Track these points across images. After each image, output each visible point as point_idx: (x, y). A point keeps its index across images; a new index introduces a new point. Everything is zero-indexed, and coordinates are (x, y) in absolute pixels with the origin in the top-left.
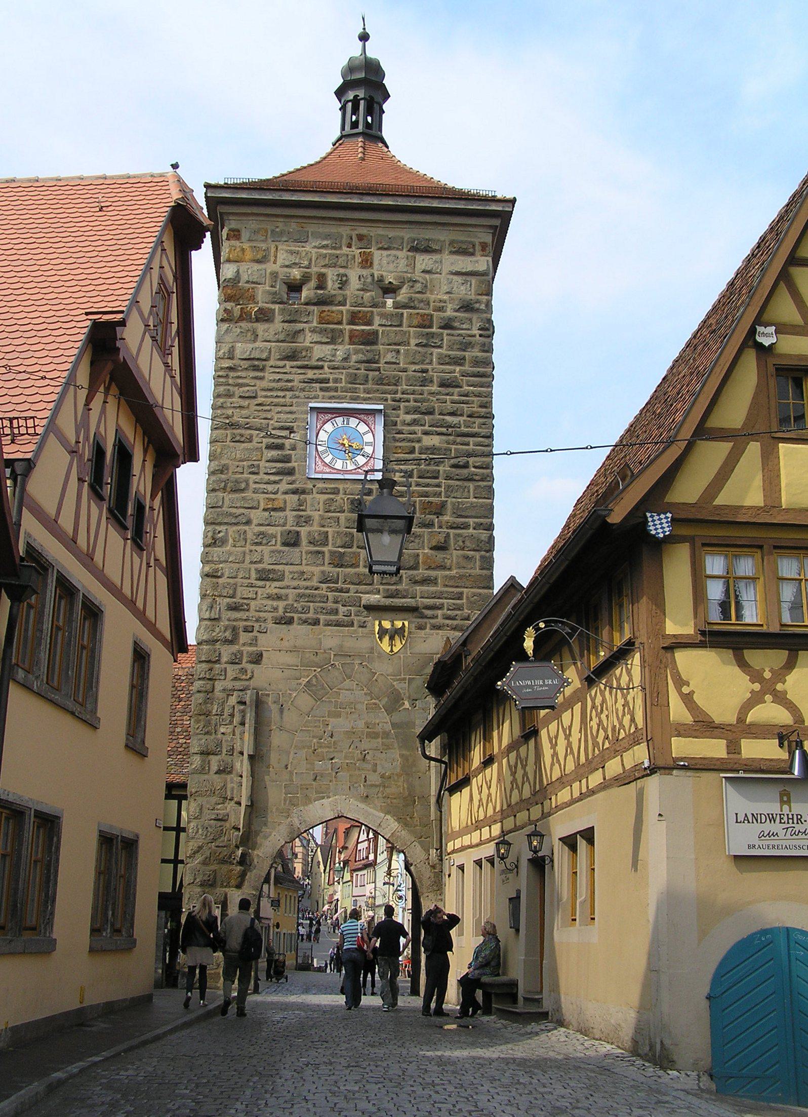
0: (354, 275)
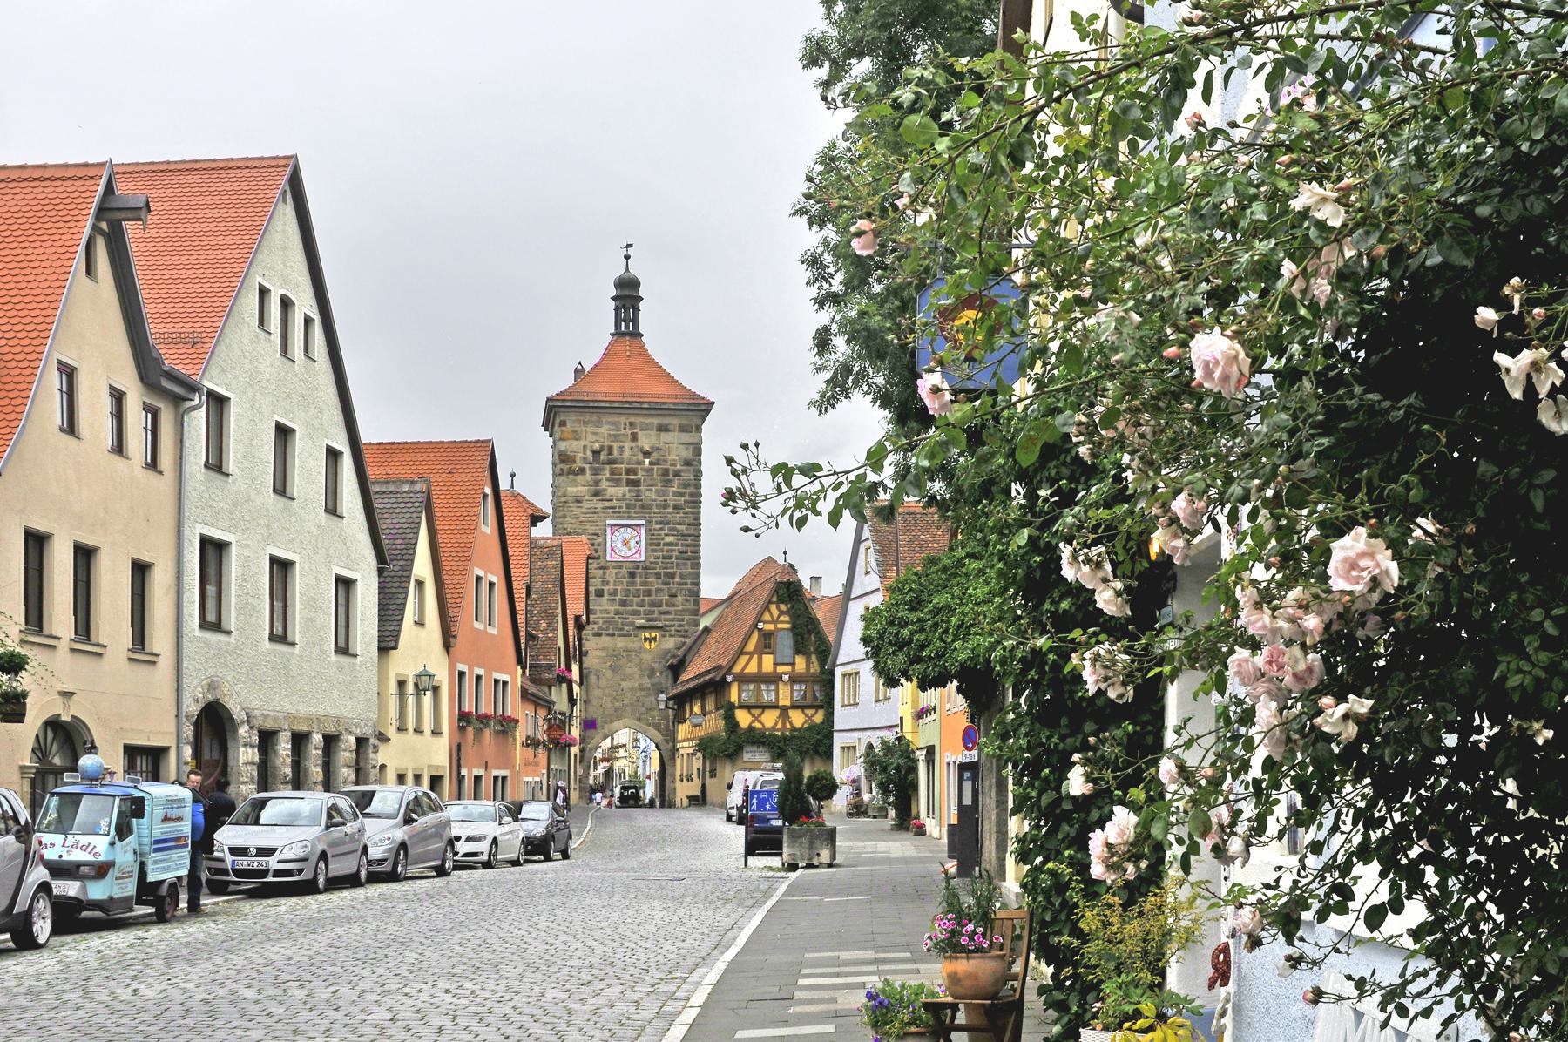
0: (627, 445)
